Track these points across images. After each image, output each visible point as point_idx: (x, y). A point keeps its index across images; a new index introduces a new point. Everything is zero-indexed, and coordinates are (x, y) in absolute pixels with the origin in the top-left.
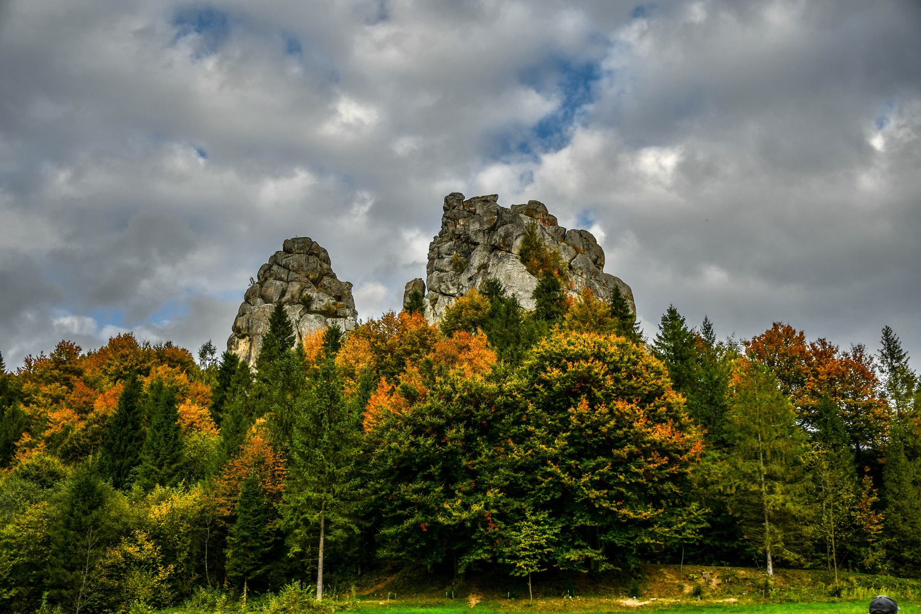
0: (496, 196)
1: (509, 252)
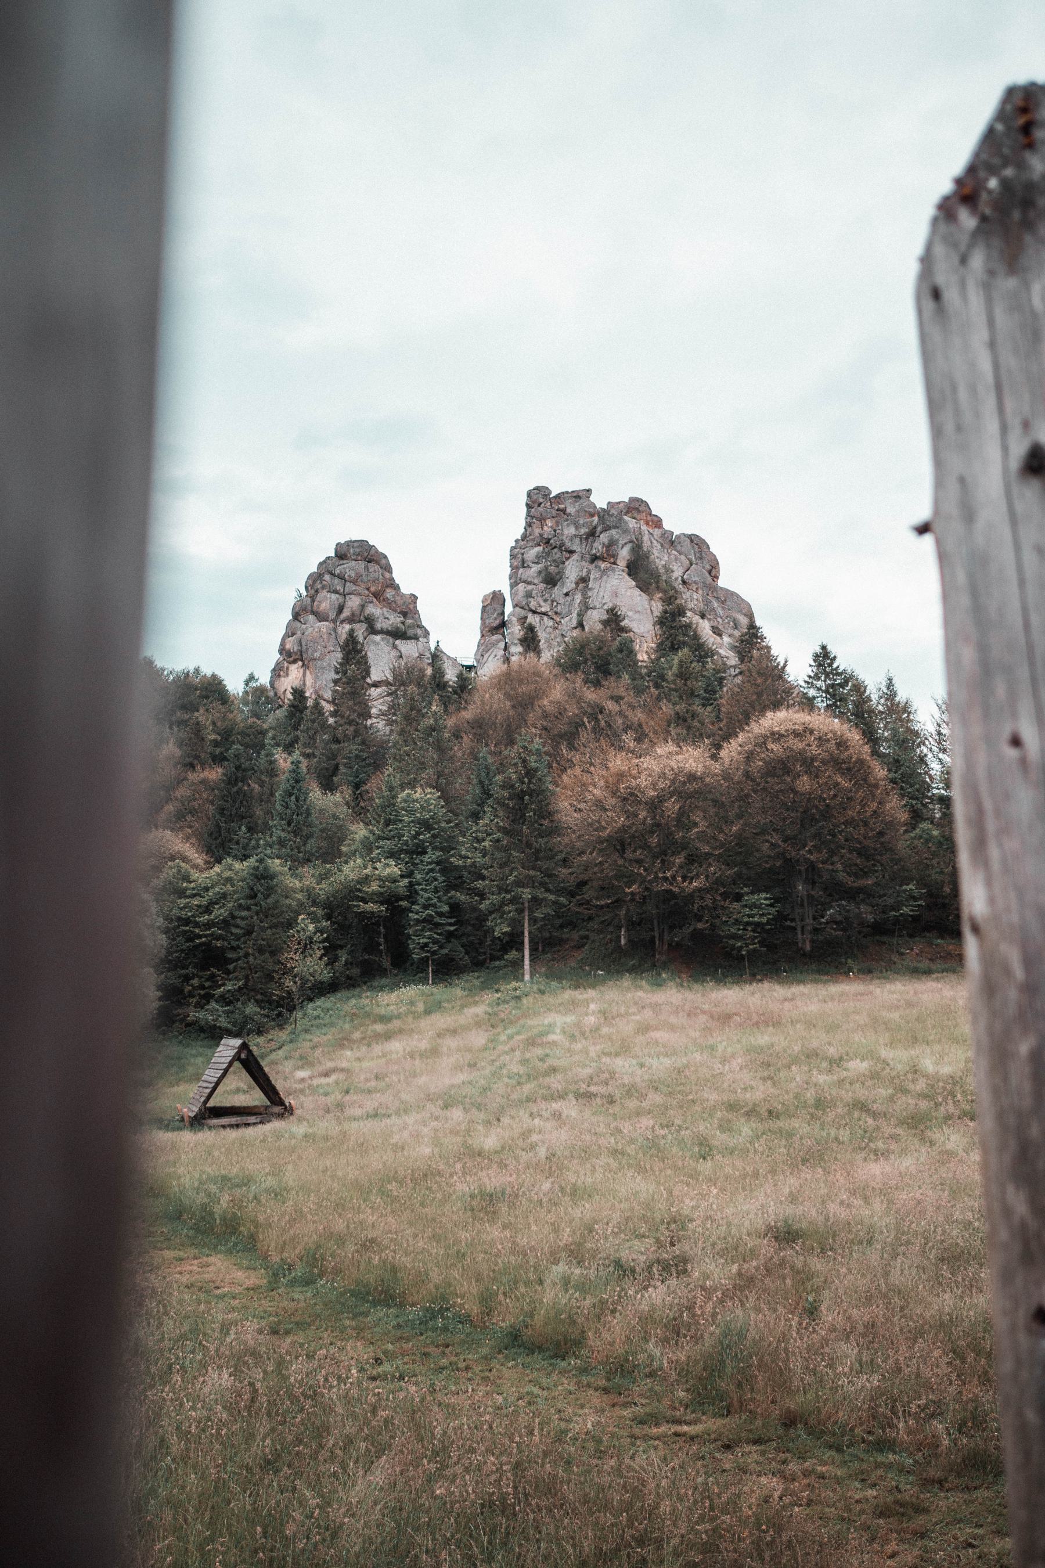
0: (589, 491)
1: (614, 563)
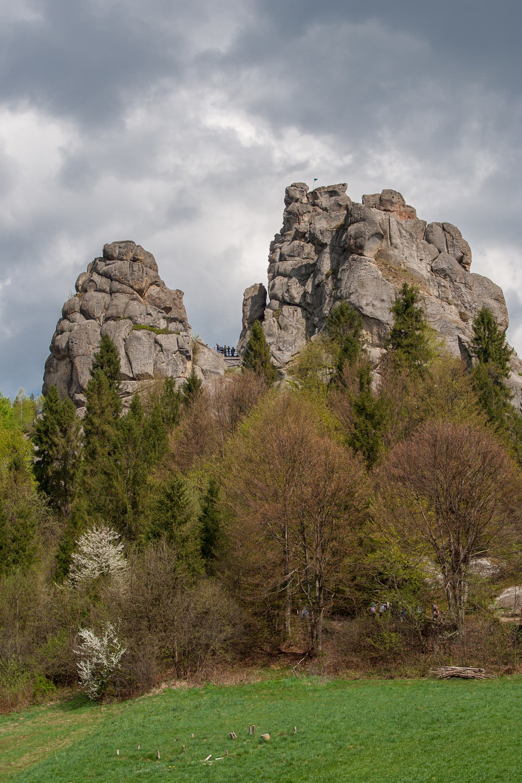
1: (361, 255)
